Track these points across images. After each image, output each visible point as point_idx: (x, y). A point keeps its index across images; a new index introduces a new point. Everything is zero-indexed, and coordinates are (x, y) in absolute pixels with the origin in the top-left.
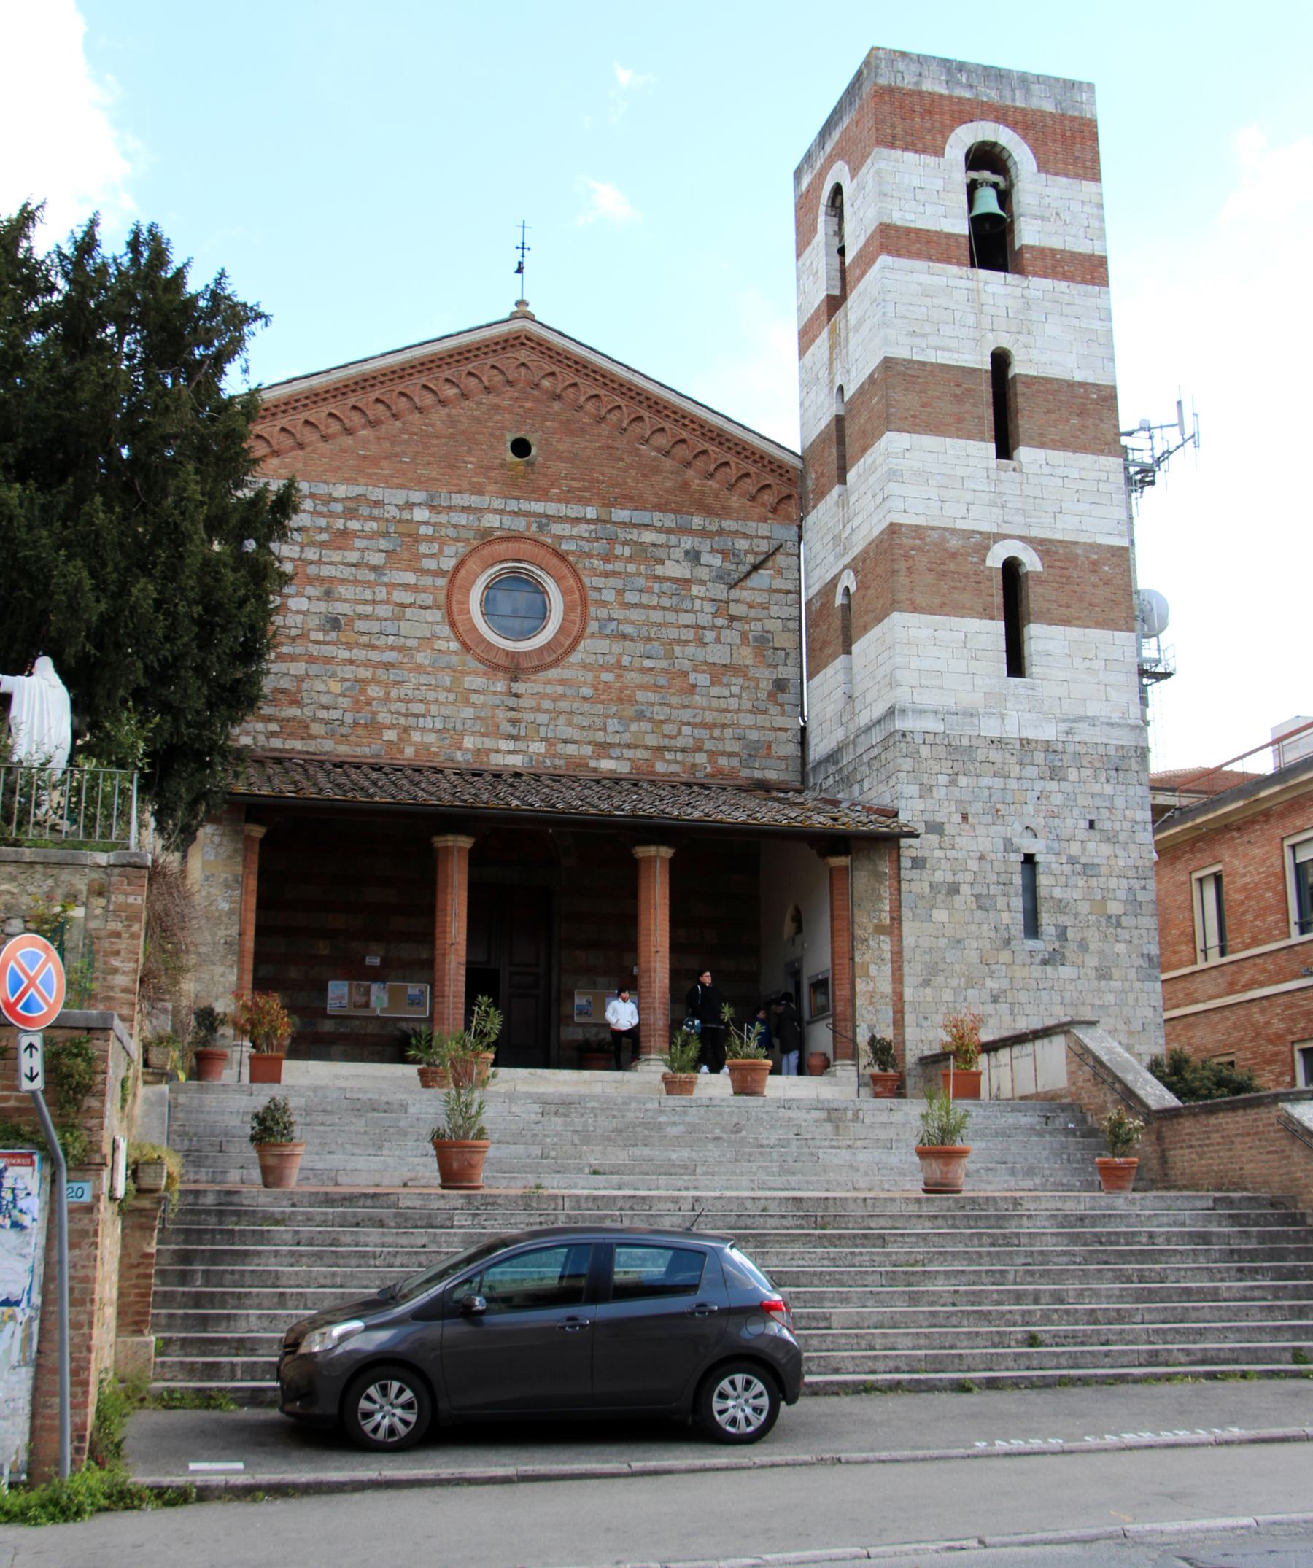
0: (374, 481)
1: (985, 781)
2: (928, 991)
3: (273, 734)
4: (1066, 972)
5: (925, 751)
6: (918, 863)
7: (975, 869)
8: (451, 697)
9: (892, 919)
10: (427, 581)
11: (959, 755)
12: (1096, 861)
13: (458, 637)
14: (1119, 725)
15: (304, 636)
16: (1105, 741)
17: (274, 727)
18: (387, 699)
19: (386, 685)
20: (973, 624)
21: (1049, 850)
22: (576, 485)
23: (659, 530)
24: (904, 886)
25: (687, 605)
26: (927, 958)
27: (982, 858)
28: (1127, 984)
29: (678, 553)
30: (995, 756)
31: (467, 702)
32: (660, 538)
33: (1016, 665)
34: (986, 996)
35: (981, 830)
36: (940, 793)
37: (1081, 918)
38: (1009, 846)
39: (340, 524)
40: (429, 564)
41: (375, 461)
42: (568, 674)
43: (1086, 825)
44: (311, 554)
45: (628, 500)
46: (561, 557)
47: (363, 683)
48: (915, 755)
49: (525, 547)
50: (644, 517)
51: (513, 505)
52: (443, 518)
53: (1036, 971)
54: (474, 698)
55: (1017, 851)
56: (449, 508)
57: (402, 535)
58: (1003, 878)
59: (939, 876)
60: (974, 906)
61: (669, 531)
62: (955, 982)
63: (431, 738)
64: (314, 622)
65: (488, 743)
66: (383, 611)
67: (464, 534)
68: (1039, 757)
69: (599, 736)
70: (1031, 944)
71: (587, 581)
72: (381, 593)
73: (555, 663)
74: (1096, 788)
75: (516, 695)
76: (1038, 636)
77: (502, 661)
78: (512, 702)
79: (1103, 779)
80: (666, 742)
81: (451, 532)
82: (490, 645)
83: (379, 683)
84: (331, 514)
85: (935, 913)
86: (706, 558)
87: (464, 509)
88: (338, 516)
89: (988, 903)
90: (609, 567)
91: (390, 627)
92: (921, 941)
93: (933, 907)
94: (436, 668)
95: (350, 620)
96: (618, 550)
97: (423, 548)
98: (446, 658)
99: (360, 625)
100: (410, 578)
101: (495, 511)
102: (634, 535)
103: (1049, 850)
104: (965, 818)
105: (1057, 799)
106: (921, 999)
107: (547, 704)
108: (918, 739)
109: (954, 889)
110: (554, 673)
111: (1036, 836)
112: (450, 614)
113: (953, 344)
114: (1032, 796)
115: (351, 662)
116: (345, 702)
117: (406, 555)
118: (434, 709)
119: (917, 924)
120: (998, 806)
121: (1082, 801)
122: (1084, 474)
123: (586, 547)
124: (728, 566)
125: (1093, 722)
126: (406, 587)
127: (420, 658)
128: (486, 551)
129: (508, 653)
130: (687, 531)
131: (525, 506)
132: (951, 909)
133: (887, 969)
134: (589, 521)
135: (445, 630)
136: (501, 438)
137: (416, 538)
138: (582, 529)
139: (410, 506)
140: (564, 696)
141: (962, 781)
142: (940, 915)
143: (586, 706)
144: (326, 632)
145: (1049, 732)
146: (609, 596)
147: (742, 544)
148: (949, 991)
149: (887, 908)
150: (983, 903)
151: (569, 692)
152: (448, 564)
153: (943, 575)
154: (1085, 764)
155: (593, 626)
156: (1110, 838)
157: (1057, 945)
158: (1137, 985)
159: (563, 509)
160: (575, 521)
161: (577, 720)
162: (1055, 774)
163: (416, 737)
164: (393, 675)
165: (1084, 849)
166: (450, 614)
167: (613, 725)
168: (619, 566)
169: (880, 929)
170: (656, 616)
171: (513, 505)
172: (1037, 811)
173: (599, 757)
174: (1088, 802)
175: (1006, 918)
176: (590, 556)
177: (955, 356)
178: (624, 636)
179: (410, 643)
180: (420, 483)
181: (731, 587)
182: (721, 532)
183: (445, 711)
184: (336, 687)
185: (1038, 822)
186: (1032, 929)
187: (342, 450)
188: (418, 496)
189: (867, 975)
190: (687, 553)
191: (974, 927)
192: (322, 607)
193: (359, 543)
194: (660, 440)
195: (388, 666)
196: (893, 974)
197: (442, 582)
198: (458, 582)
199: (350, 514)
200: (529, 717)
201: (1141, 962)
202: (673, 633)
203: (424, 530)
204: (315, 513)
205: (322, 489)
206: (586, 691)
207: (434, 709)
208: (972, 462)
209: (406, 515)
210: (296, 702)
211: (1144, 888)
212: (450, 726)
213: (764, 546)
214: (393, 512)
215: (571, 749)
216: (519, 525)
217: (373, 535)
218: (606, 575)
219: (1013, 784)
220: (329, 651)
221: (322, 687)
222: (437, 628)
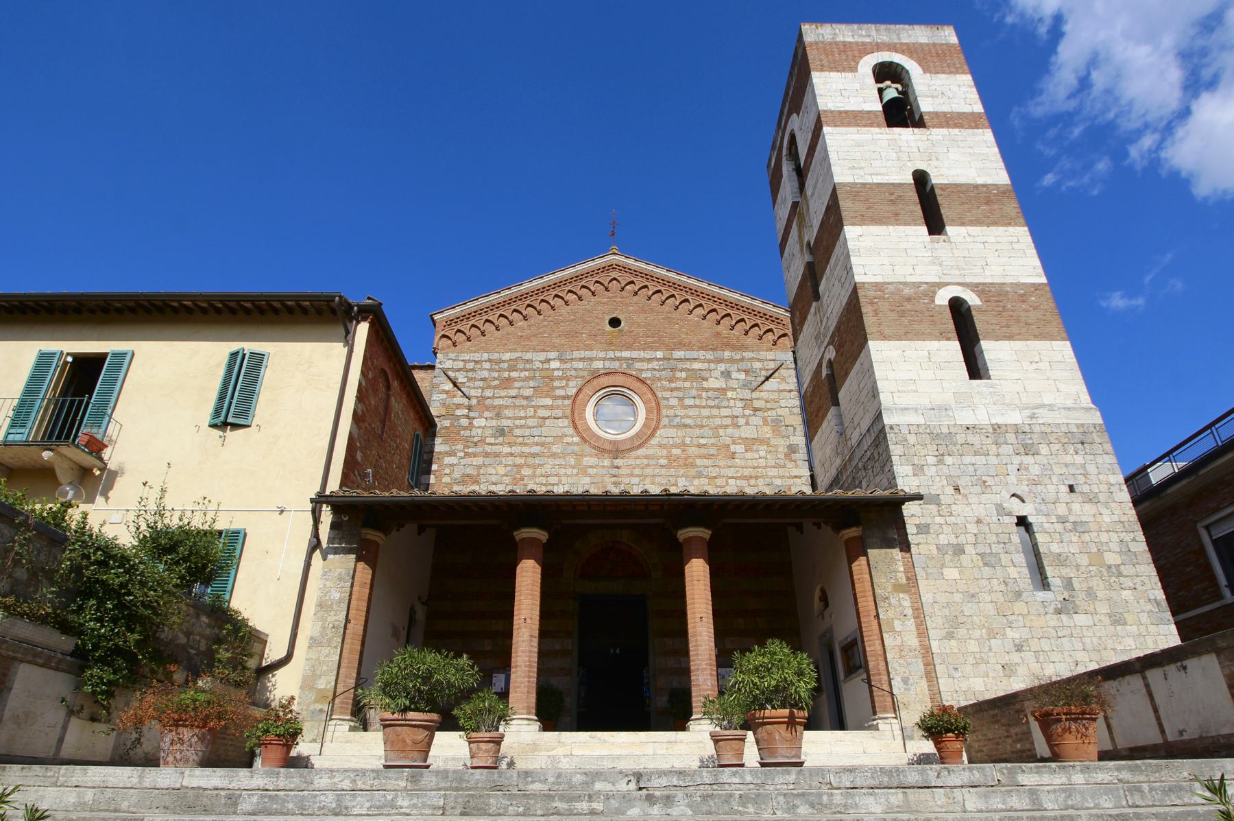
0: (527, 349)
2: (953, 642)
6: (923, 529)
7: (975, 531)
8: (575, 471)
9: (908, 579)
10: (560, 402)
12: (1084, 519)
13: (579, 434)
14: (1074, 409)
16: (1065, 421)
18: (534, 476)
19: (535, 467)
21: (1038, 512)
22: (650, 340)
23: (702, 361)
25: (725, 403)
26: (946, 612)
27: (979, 522)
29: (717, 374)
31: (585, 474)
32: (706, 365)
34: (1010, 646)
39: (506, 374)
41: (528, 338)
42: (651, 452)
43: (1065, 489)
44: (488, 393)
45: (681, 345)
46: (642, 381)
47: (520, 466)
49: (619, 380)
50: (694, 354)
51: (611, 355)
52: (568, 366)
54: (590, 471)
55: (1010, 514)
56: (572, 360)
57: (543, 377)
59: (943, 539)
60: (981, 564)
61: (709, 361)
62: (977, 633)
64: (489, 432)
66: (531, 422)
67: (581, 373)
68: (1011, 437)
70: (1041, 595)
71: (659, 394)
72: (531, 412)
74: (1068, 459)
75: (618, 467)
77: (607, 447)
78: (614, 471)
79: (1072, 452)
81: (573, 373)
82: (599, 438)
83: (529, 466)
85: (946, 571)
86: (735, 375)
87: (581, 360)
88: (505, 370)
90: (673, 385)
91: (536, 432)
92: (938, 598)
93: (943, 566)
94: (565, 455)
95: (511, 429)
96: (678, 375)
97: (556, 384)
98: (572, 447)
99: (517, 432)
100: (548, 401)
101: (600, 359)
102: (688, 365)
103: (1038, 512)
106: (948, 651)
107: (637, 471)
109: (959, 550)
111: (1023, 501)
112: (573, 421)
114: (1012, 469)
115: (512, 454)
116: (507, 480)
117: (546, 389)
118: (564, 479)
119: (932, 582)
120: (984, 478)
121: (1057, 470)
123: (658, 374)
124: (750, 378)
125: (1051, 407)
126: (545, 407)
127: (555, 449)
128: (595, 382)
130: (721, 361)
131: (618, 354)
132: (960, 567)
133: (911, 623)
134: (659, 360)
135: (571, 431)
136: (603, 319)
137: (552, 379)
138: (655, 365)
139: (548, 361)
140: (648, 465)
142: (951, 573)
144: (496, 438)
145: (1015, 418)
147: (757, 365)
148: (972, 642)
149: (902, 569)
150: (988, 560)
151: (652, 462)
152: (573, 391)
154: (1052, 439)
155: (665, 421)
156: (1092, 499)
159: (642, 354)
160: (650, 360)
161: (658, 480)
162: (1029, 450)
165: (1070, 510)
166: (573, 421)
169: (898, 588)
170: (706, 412)
171: (611, 355)
174: (1064, 470)
176: (660, 379)
178: (686, 426)
179: (548, 440)
180: (554, 347)
181: (753, 391)
182: (742, 360)
183: (570, 480)
184: (501, 470)
185: (1022, 490)
187: (508, 334)
188: (553, 355)
189: (893, 630)
190: (722, 373)
191: (984, 582)
192: (494, 423)
193: (517, 384)
194: (699, 311)
195: (534, 455)
196: (918, 626)
198: (577, 402)
199: (511, 369)
200: (626, 480)
202: (718, 422)
203: (556, 373)
205: (496, 356)
206: (663, 462)
207: (564, 479)
209: (546, 366)
210: (476, 482)
213: (772, 365)
216: (615, 365)
218: (672, 390)
220: (496, 449)
221: (493, 471)
222: (565, 430)
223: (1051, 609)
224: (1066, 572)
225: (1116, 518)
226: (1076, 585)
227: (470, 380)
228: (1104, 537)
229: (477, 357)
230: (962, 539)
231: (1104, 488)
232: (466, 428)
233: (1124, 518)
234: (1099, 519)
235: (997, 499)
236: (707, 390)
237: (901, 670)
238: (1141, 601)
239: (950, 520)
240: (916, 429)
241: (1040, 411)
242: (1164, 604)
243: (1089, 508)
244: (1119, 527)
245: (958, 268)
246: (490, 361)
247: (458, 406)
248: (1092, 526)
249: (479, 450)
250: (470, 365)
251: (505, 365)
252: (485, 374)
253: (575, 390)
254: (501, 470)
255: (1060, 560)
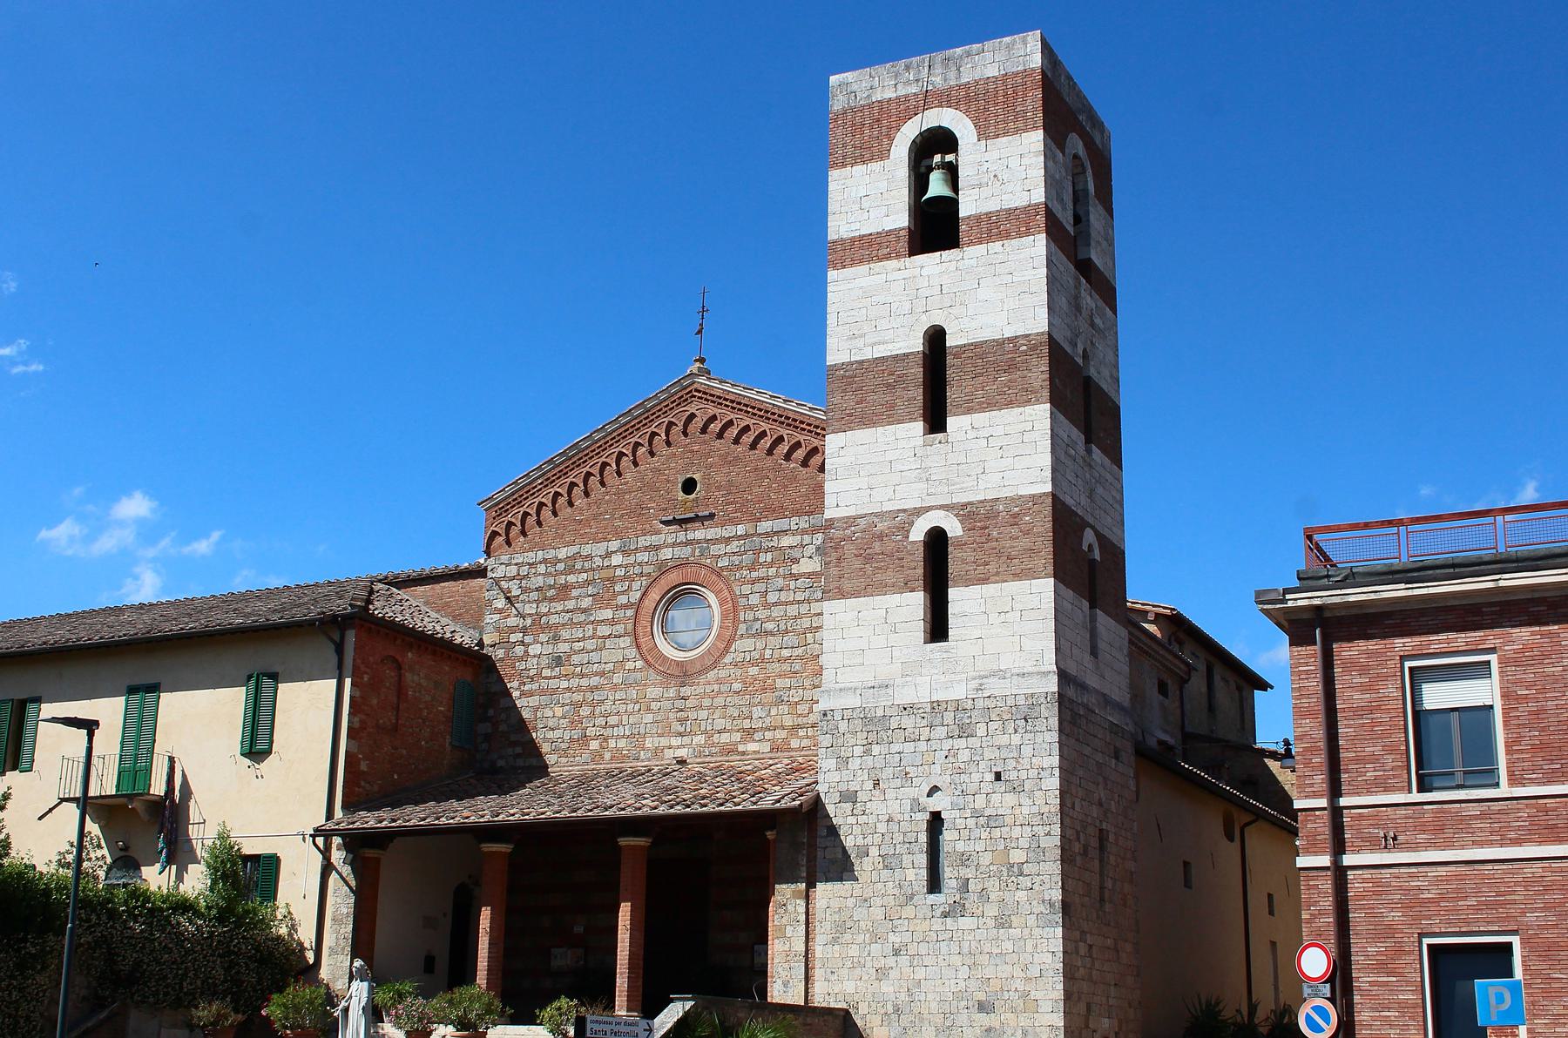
1: (895, 748)
3: (519, 755)
4: (966, 922)
5: (843, 726)
10: (621, 613)
11: (875, 725)
15: (539, 674)
17: (519, 750)
20: (893, 600)
24: (820, 853)
26: (836, 917)
28: (1026, 931)
30: (908, 722)
33: (938, 629)
34: (889, 950)
35: (891, 794)
36: (854, 764)
37: (982, 869)
38: (916, 806)
40: (623, 600)
42: (722, 674)
43: (992, 776)
44: (544, 609)
47: (578, 705)
48: (833, 732)
52: (631, 560)
53: (937, 924)
54: (654, 706)
58: (911, 837)
61: (804, 532)
62: (860, 938)
63: (622, 743)
64: (544, 661)
65: (664, 742)
67: (647, 569)
69: (747, 724)
73: (714, 665)
74: (1004, 740)
76: (959, 598)
78: (679, 704)
79: (1011, 730)
80: (800, 721)
84: (558, 573)
89: (894, 862)
90: (754, 575)
91: (595, 657)
99: (575, 659)
104: (876, 784)
105: (964, 756)
108: (838, 716)
110: (711, 675)
113: (889, 335)
114: (941, 755)
118: (625, 718)
121: (988, 754)
122: (1008, 430)
125: (1000, 674)
129: (677, 663)
134: (739, 538)
135: (633, 652)
137: (612, 580)
139: (609, 555)
141: (876, 749)
143: (736, 700)
145: (959, 692)
146: (755, 599)
151: (724, 688)
153: (869, 559)
155: (742, 628)
157: (957, 898)
158: (1037, 932)
160: (728, 540)
161: (730, 711)
162: (965, 732)
163: (612, 744)
164: (597, 696)
167: (757, 712)
168: (762, 573)
170: (792, 610)
172: (944, 770)
173: (743, 741)
175: (911, 875)
176: (739, 567)
177: (890, 346)
180: (617, 534)
184: (559, 712)
186: (934, 884)
188: (614, 545)
191: (880, 886)
192: (549, 649)
193: (575, 593)
195: (592, 689)
197: (630, 613)
199: (570, 570)
200: (692, 715)
201: (1042, 908)
204: (546, 574)
205: (551, 554)
206: (737, 686)
208: (902, 444)
211: (1048, 834)
212: (635, 731)
214: (598, 561)
215: (725, 738)
217: (588, 583)
219: (922, 746)
220: (553, 683)
223: (938, 913)
224: (968, 873)
225: (1035, 809)
226: (971, 887)
227: (525, 590)
228: (1016, 832)
229: (530, 557)
230: (869, 840)
231: (1033, 773)
232: (521, 659)
233: (1045, 809)
234: (1017, 812)
235: (911, 792)
236: (796, 577)
237: (783, 974)
238: (1035, 903)
239: (863, 819)
240: (848, 715)
241: (990, 680)
242: (1058, 905)
243: (1010, 799)
244: (1036, 820)
245: (948, 482)
246: (545, 561)
247: (513, 630)
248: (1008, 820)
249: (535, 686)
250: (524, 570)
251: (561, 566)
252: (540, 581)
253: (638, 595)
254: (559, 712)
255: (964, 860)
